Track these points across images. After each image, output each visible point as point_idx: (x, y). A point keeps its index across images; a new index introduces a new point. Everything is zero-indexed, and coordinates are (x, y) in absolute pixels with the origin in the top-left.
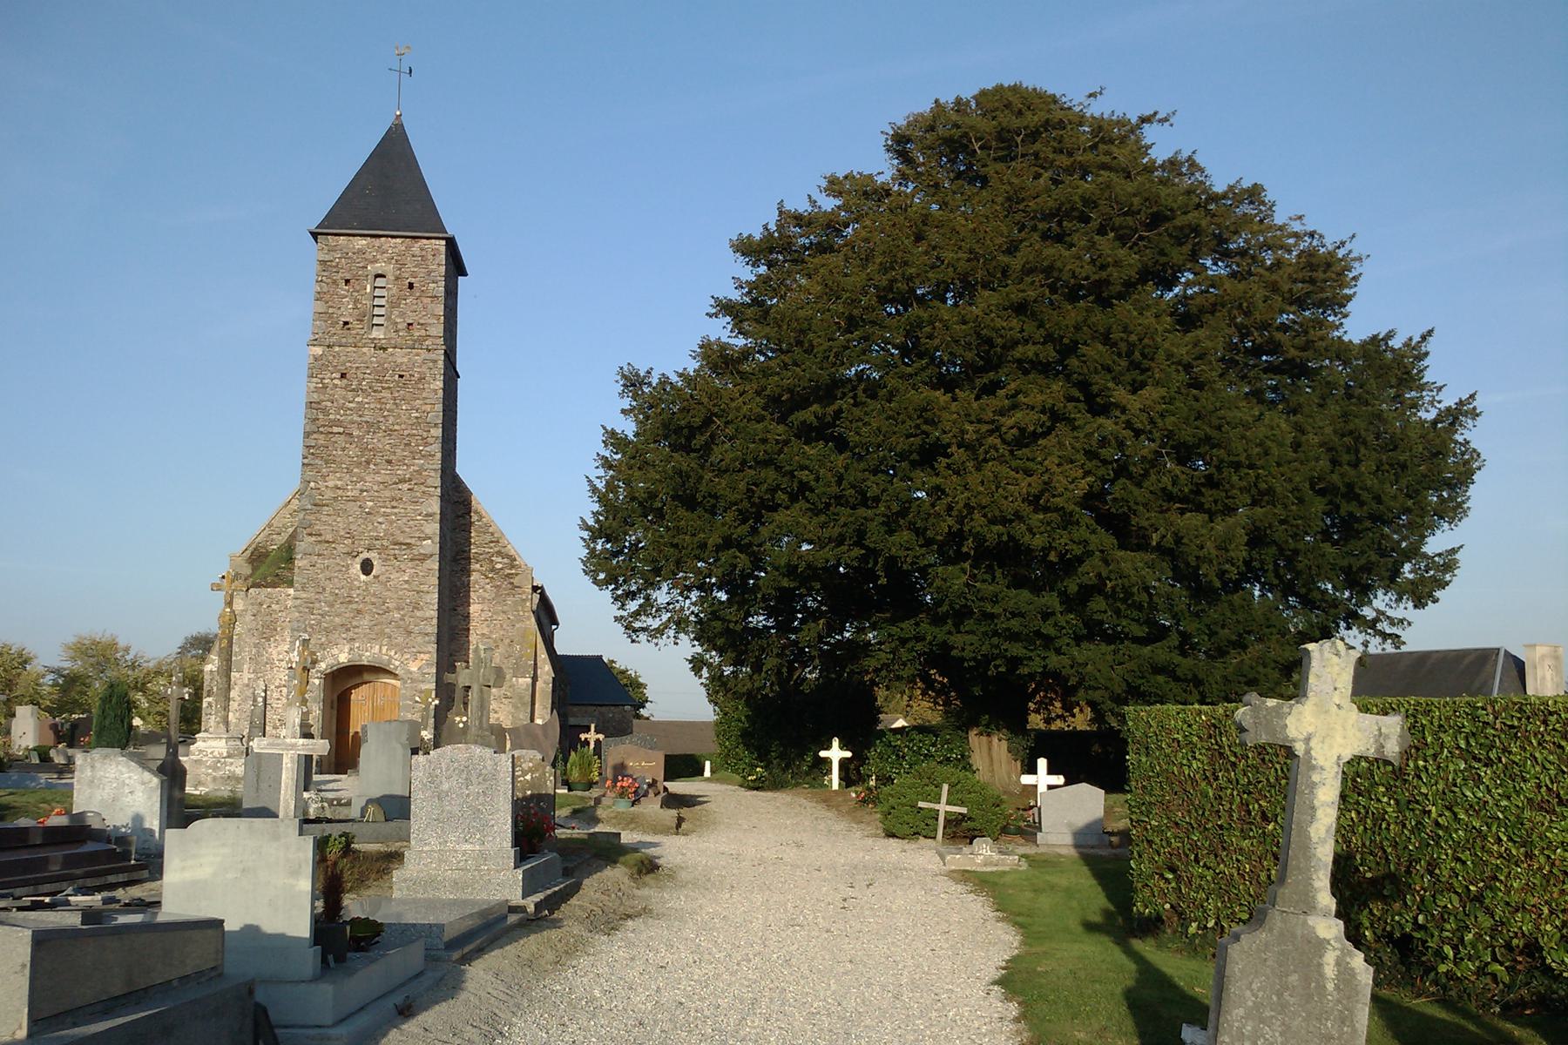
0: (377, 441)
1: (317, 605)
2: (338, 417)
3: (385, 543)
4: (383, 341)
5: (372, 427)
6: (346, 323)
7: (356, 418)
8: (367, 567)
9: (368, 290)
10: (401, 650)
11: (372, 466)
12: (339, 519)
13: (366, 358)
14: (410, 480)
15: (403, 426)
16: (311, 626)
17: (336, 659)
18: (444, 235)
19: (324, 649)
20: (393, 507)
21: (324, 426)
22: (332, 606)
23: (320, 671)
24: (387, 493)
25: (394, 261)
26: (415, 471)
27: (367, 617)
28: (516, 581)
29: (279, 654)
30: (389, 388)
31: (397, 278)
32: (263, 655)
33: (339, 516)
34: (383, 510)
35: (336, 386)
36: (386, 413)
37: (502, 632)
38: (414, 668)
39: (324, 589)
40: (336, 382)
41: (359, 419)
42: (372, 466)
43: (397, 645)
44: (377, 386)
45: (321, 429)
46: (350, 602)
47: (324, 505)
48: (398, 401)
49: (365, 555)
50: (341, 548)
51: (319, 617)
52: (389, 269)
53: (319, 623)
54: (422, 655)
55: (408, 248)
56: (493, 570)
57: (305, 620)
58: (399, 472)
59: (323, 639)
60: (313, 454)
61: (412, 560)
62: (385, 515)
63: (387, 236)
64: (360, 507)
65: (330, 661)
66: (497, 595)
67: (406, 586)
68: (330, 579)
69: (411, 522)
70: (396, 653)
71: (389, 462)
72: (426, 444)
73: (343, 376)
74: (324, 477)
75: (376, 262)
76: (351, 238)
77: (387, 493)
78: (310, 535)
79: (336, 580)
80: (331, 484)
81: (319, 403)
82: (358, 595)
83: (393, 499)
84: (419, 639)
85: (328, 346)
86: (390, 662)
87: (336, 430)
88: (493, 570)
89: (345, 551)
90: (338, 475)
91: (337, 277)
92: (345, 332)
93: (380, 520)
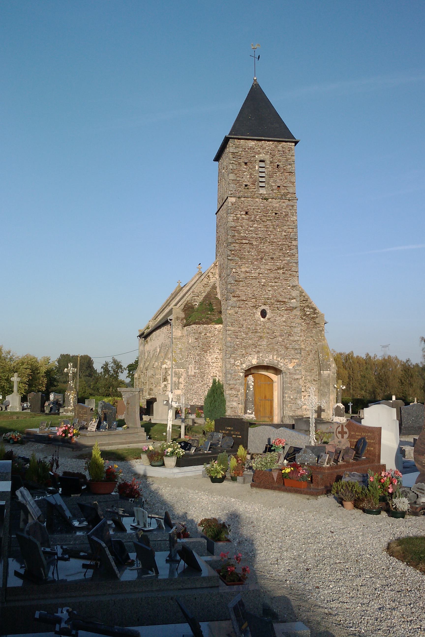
0: (266, 247)
1: (239, 334)
2: (245, 234)
3: (272, 301)
4: (266, 195)
5: (262, 240)
6: (246, 186)
7: (254, 235)
8: (264, 314)
9: (257, 168)
10: (284, 358)
11: (264, 261)
12: (248, 289)
13: (257, 204)
14: (283, 268)
15: (279, 240)
16: (237, 345)
17: (251, 362)
18: (294, 140)
19: (244, 357)
20: (276, 282)
21: (238, 239)
22: (247, 334)
23: (243, 369)
24: (272, 275)
25: (269, 154)
26: (285, 263)
27: (265, 340)
28: (317, 320)
29: (212, 359)
30: (270, 220)
31: (271, 162)
32: (203, 360)
33: (248, 287)
34: (270, 284)
35: (243, 218)
36: (269, 233)
37: (311, 347)
38: (291, 367)
39: (243, 326)
40: (243, 216)
41: (256, 236)
42: (264, 261)
43: (281, 355)
44: (264, 219)
45: (237, 241)
46: (256, 332)
47: (240, 281)
48: (275, 227)
49: (263, 307)
50: (250, 304)
51: (241, 340)
52: (267, 158)
53: (241, 343)
54: (294, 360)
55: (276, 146)
56: (305, 315)
57: (234, 342)
58: (278, 264)
59: (244, 352)
60: (233, 254)
61: (286, 310)
62: (272, 286)
63: (265, 140)
64: (259, 282)
65: (248, 363)
66: (308, 328)
67: (284, 324)
68: (245, 320)
69: (285, 290)
70: (281, 359)
71: (272, 258)
72: (290, 249)
73: (247, 213)
74: (240, 267)
75: (260, 153)
76: (247, 141)
77: (272, 275)
78: (234, 296)
79: (249, 321)
80: (243, 270)
81: (235, 227)
82: (260, 328)
83: (275, 278)
84: (293, 352)
85: (239, 198)
86: (278, 363)
87: (244, 241)
88: (305, 315)
89: (252, 305)
90: (247, 265)
91: (241, 161)
92: (246, 190)
93: (269, 289)
